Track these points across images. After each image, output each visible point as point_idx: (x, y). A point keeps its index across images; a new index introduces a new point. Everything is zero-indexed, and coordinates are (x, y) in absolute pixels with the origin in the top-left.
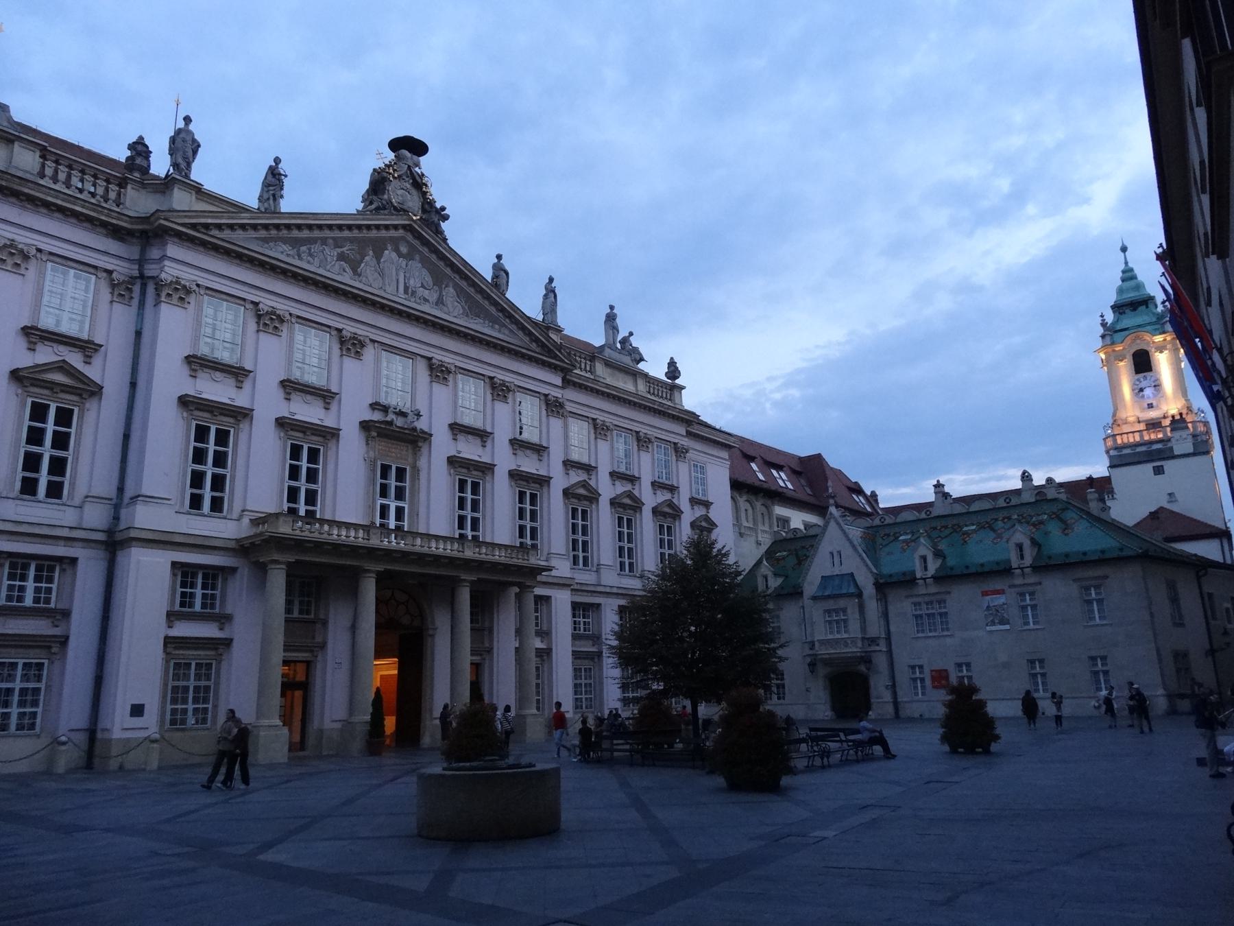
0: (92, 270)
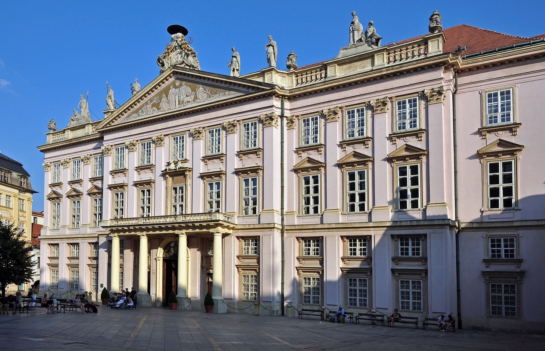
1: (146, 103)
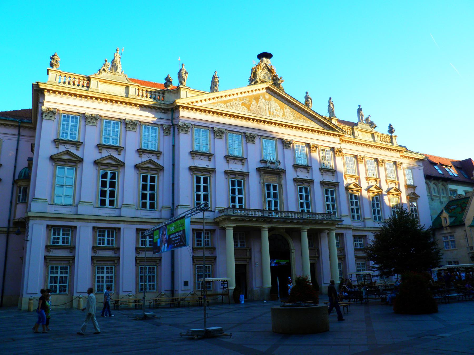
0: (157, 126)
1: (236, 100)
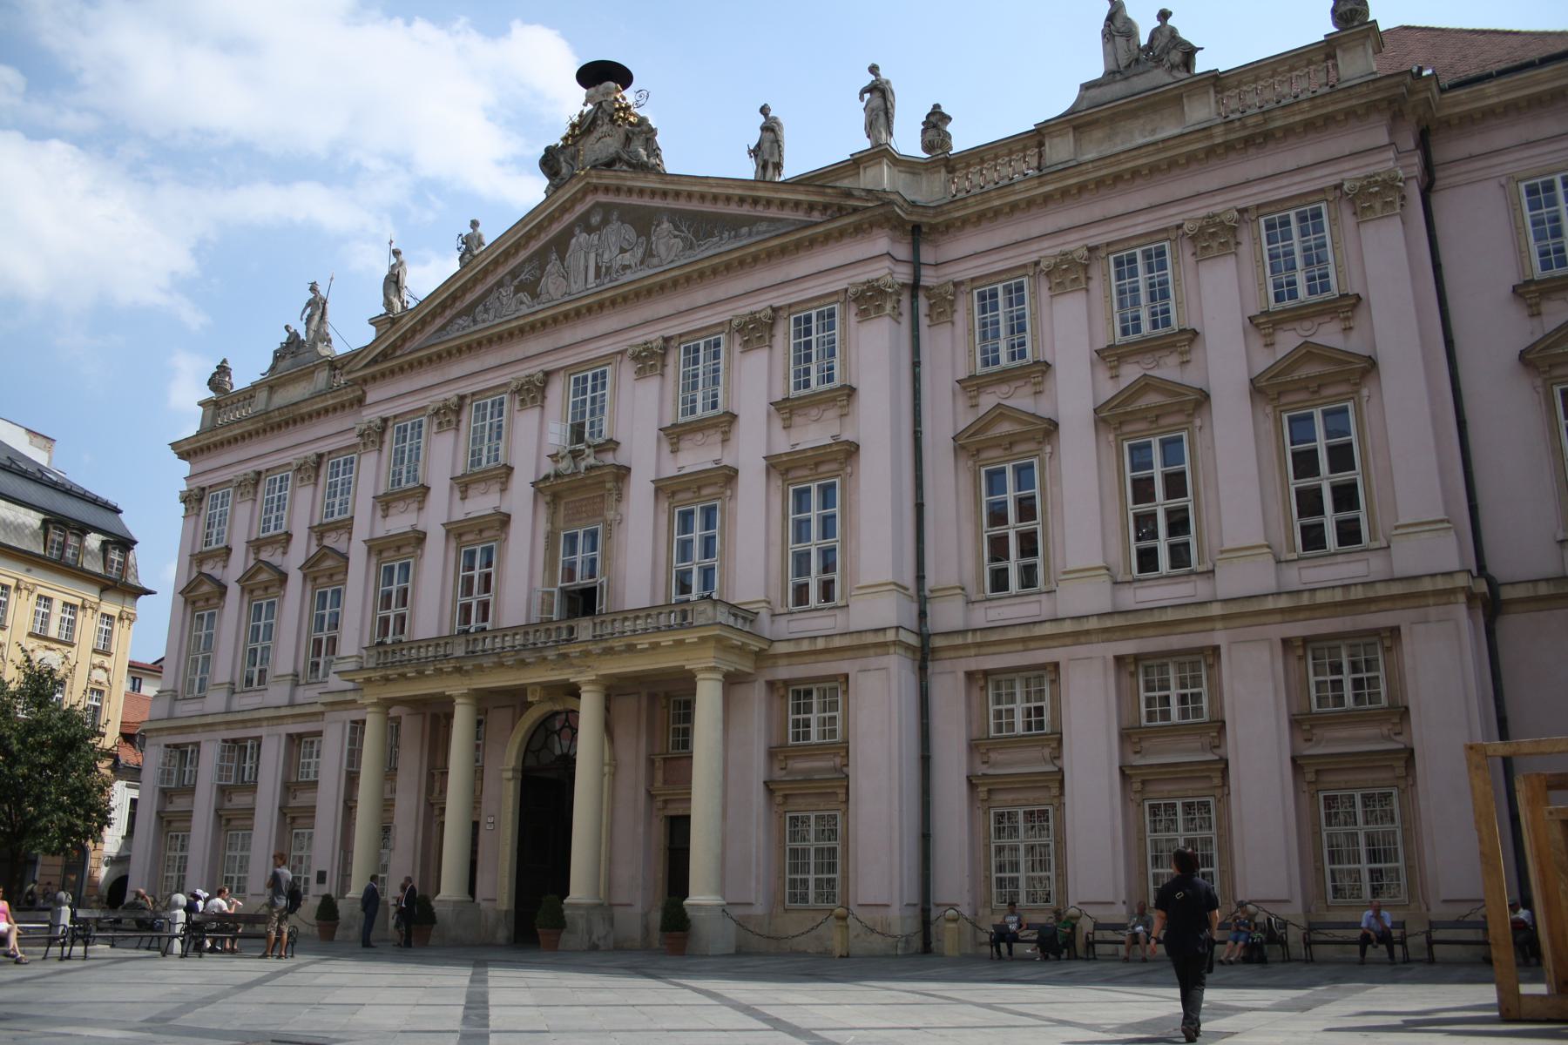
1: (500, 284)
